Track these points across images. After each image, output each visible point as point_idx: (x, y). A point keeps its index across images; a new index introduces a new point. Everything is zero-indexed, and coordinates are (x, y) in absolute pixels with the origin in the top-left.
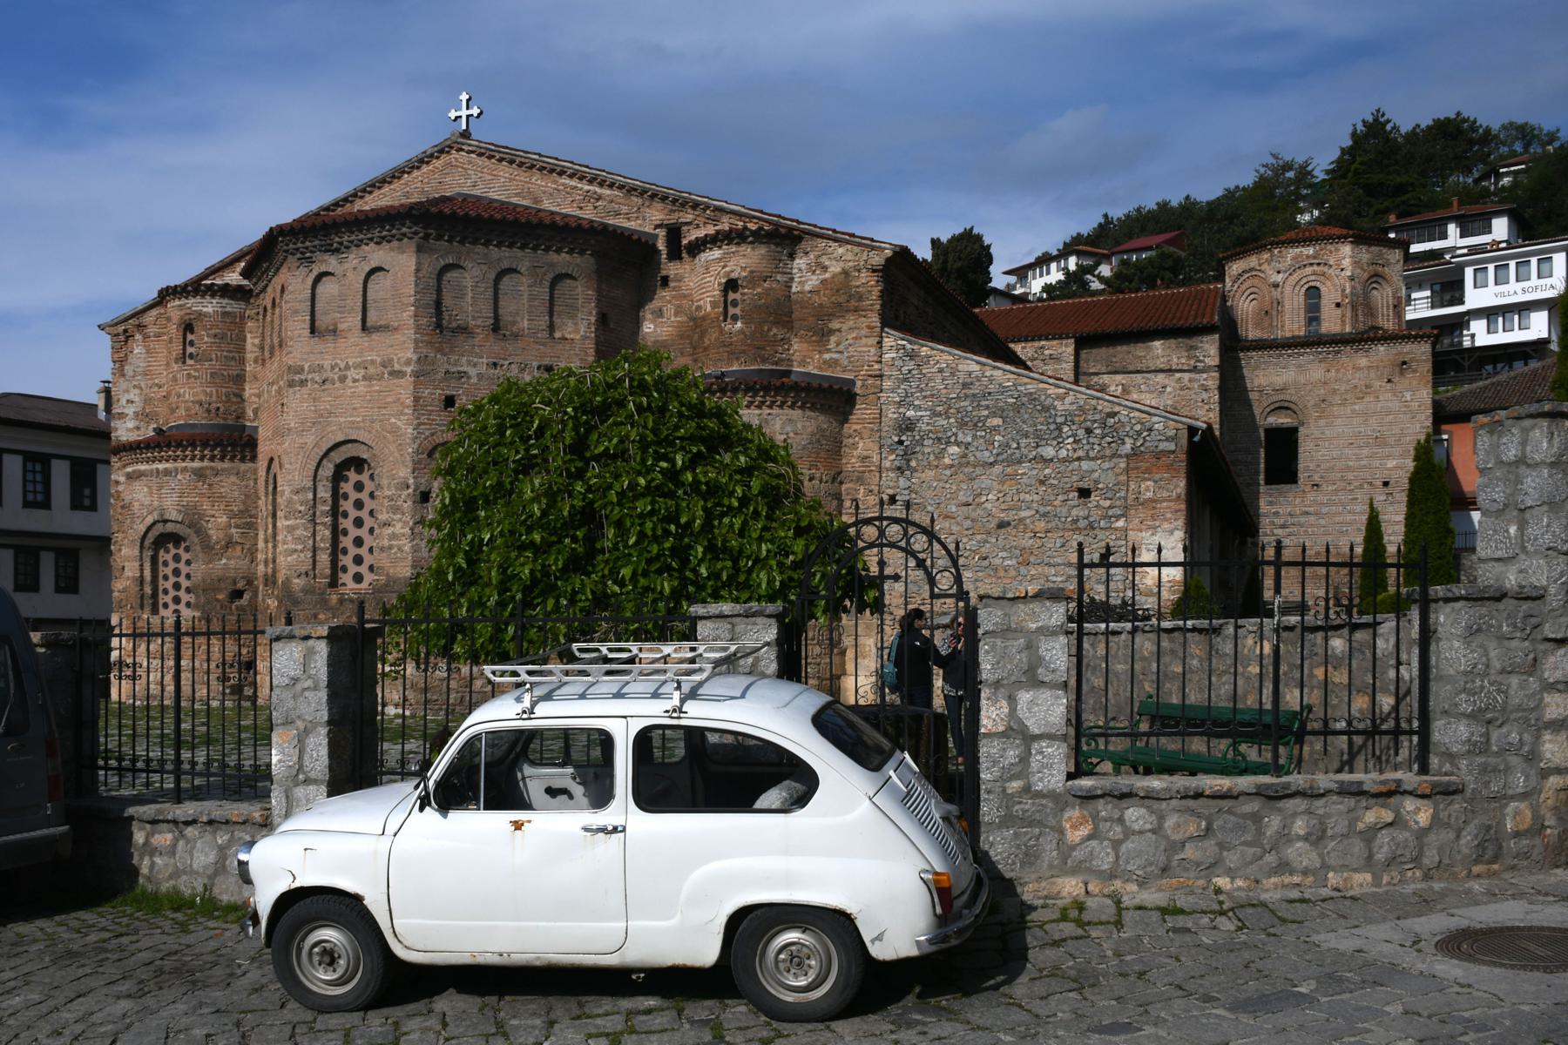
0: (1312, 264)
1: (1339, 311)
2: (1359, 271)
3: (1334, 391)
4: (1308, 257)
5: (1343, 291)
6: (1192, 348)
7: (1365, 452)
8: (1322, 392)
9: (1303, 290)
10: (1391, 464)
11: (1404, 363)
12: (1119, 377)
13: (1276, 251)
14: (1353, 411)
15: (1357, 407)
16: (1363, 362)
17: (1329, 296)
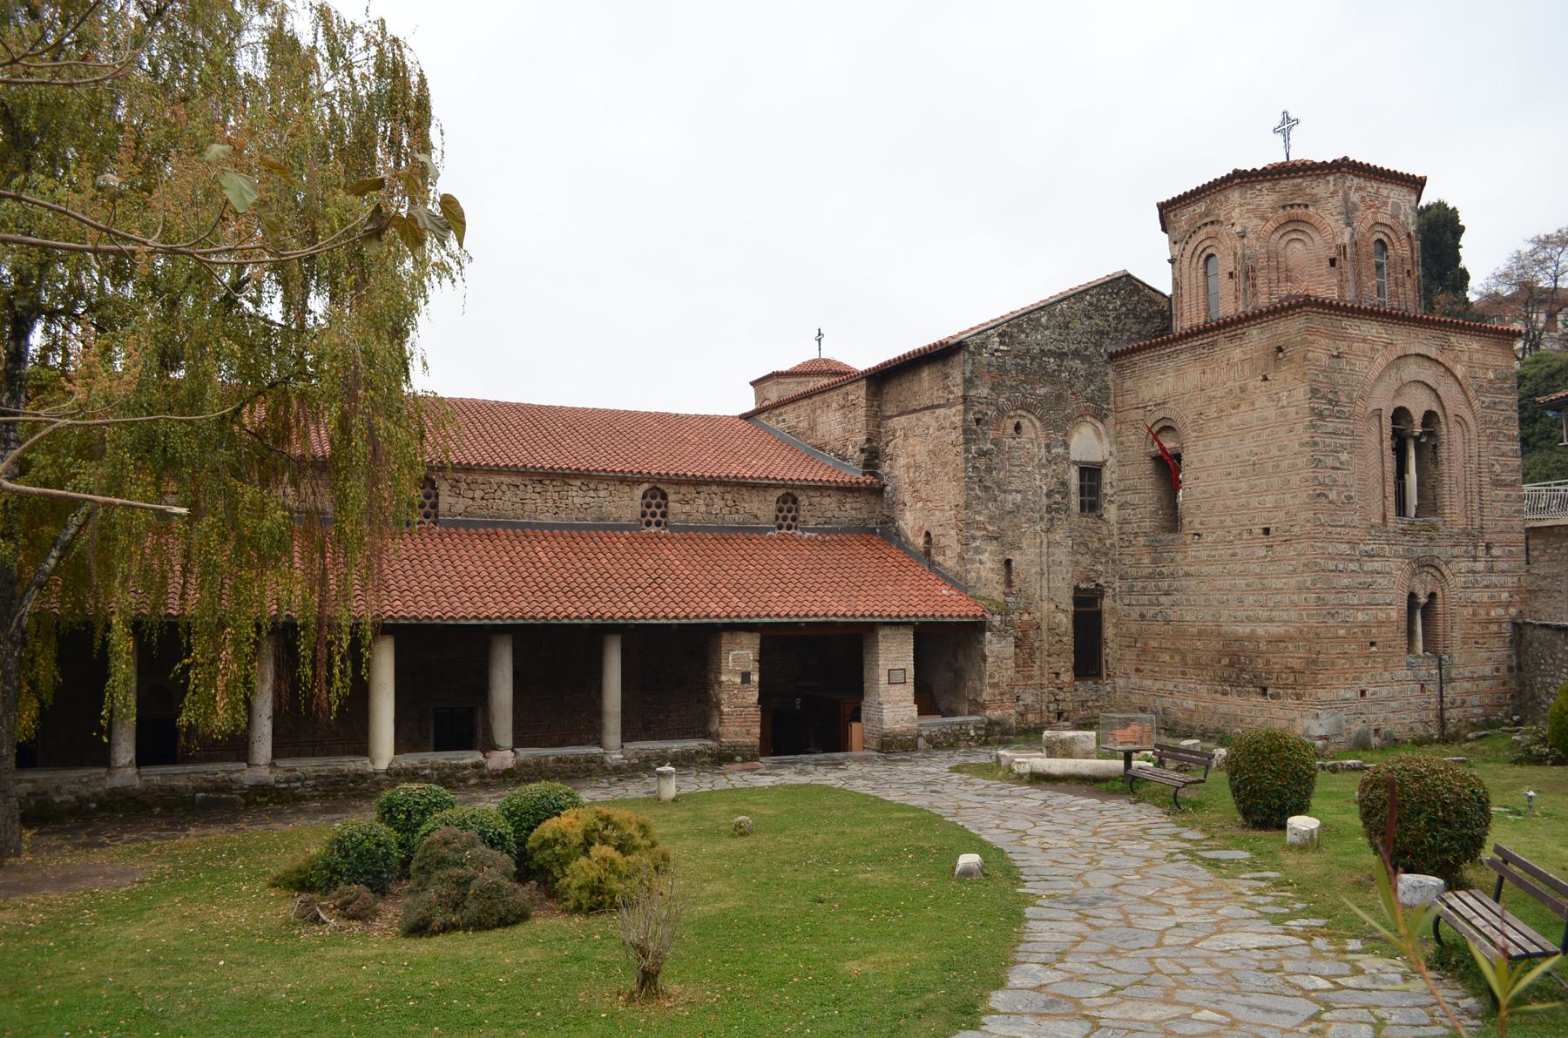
0: (1206, 224)
1: (1232, 283)
2: (1256, 221)
3: (1211, 399)
4: (1201, 216)
5: (1235, 254)
6: (947, 376)
7: (1244, 485)
8: (1199, 403)
9: (1202, 260)
10: (1270, 500)
11: (1280, 349)
12: (903, 419)
13: (1172, 215)
14: (1230, 426)
15: (1233, 420)
16: (1237, 354)
17: (1224, 263)
